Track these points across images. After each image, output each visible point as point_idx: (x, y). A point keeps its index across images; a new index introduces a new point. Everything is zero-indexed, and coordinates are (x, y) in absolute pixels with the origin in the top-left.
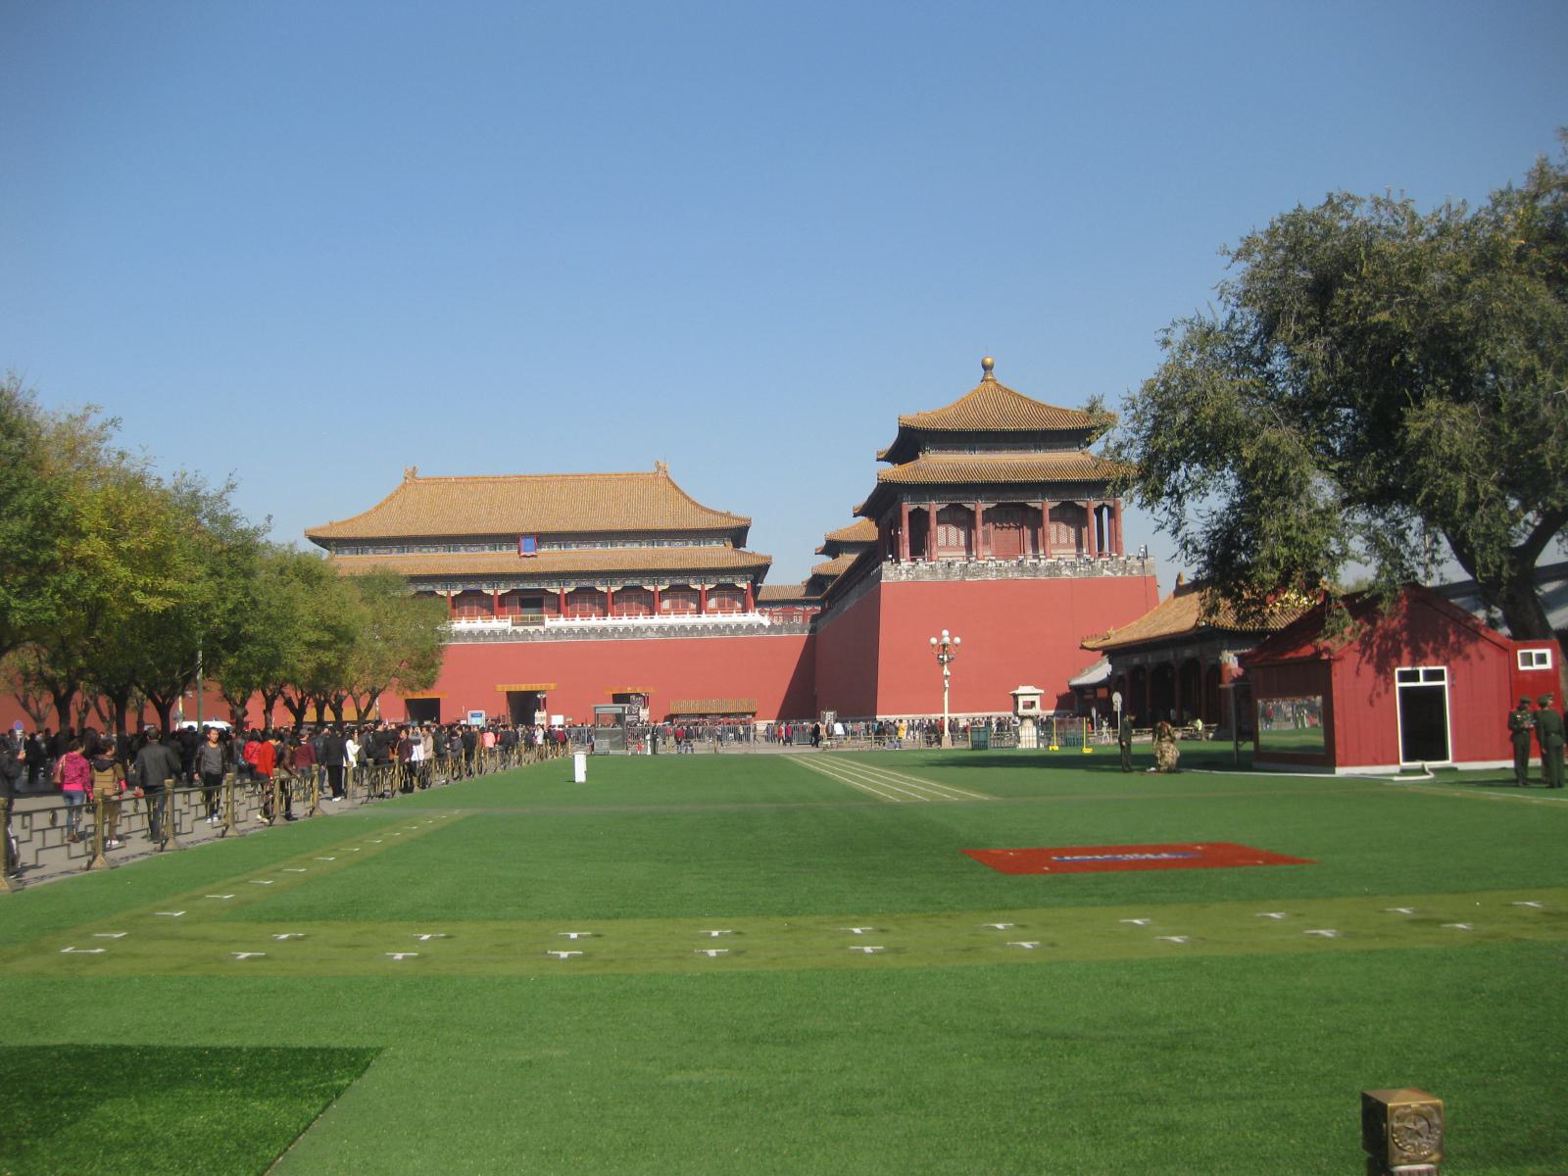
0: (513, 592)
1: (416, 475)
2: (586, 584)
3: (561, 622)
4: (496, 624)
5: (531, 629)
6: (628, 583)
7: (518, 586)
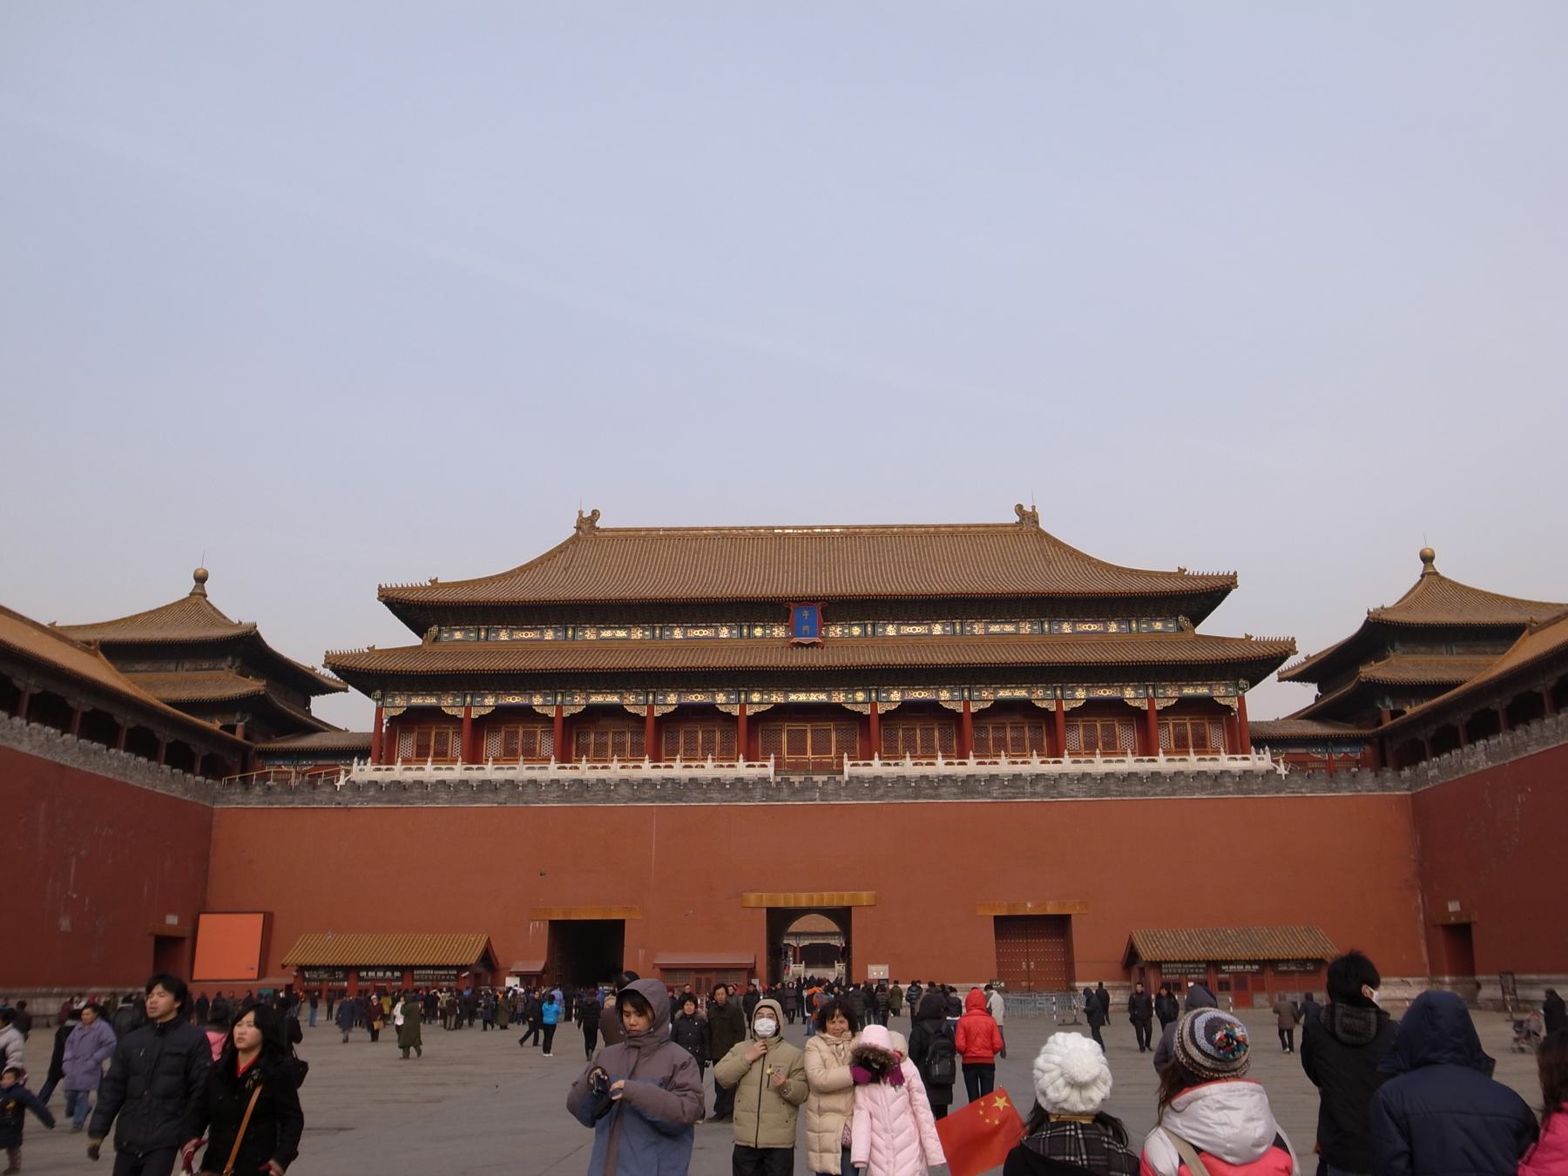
3: (877, 767)
4: (742, 769)
5: (820, 779)
6: (1004, 694)
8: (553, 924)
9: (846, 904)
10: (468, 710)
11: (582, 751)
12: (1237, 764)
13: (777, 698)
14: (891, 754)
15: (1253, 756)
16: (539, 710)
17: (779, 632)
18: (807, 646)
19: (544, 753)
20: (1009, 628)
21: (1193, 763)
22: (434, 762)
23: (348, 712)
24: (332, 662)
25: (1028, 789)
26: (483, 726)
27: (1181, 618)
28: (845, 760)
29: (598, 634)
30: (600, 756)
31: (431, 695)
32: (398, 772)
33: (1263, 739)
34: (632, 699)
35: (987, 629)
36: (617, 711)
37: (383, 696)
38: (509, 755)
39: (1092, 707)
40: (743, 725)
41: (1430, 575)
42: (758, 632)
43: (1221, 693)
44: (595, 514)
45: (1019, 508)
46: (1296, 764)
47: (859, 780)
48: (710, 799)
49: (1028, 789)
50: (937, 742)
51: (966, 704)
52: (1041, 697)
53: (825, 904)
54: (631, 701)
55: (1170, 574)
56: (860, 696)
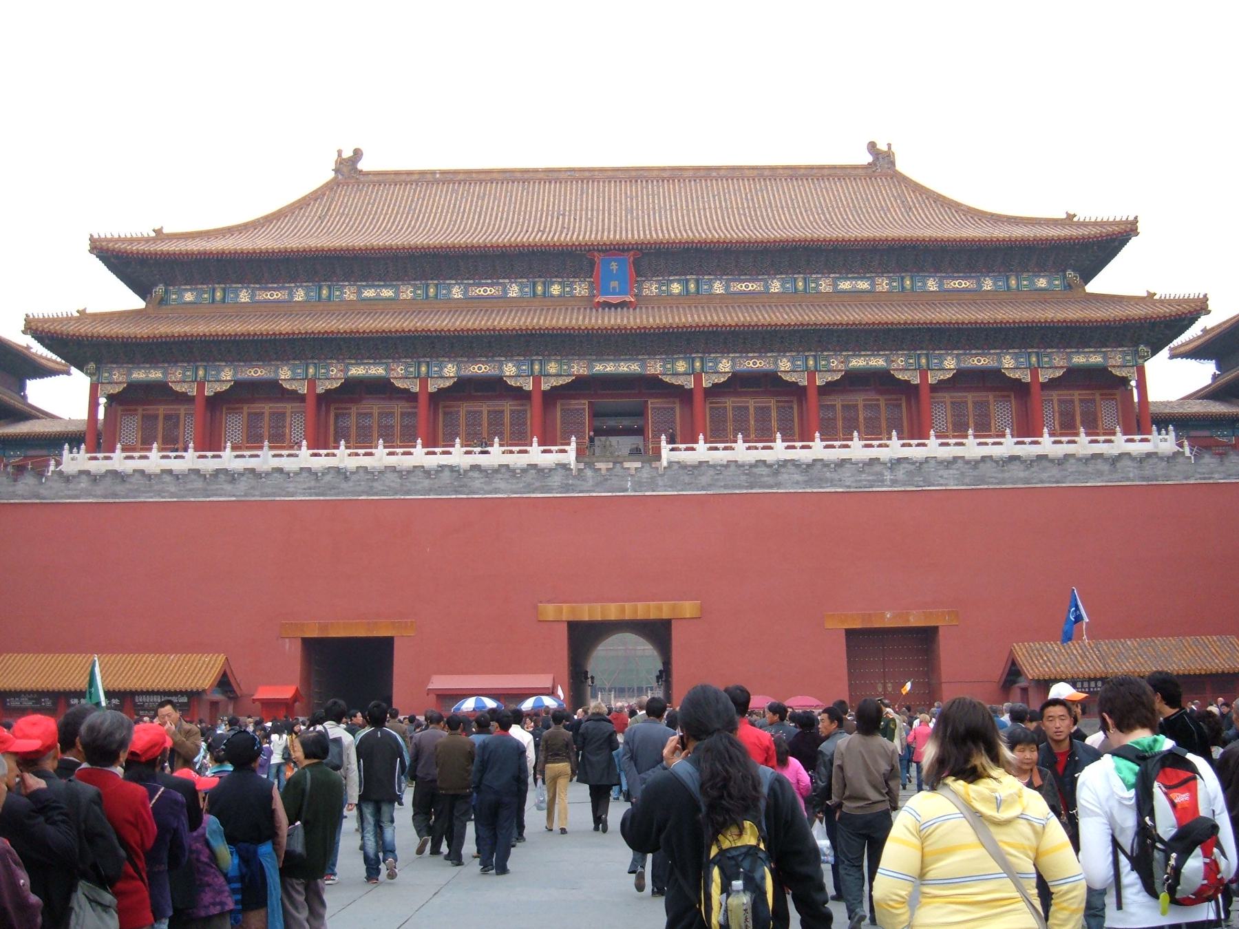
0: (580, 386)
1: (363, 165)
2: (754, 364)
3: (701, 451)
4: (536, 454)
6: (858, 363)
7: (590, 367)
8: (307, 642)
9: (665, 616)
10: (201, 386)
12: (1138, 447)
13: (579, 368)
14: (718, 435)
15: (1154, 436)
16: (287, 386)
17: (581, 289)
18: (616, 306)
19: (295, 437)
20: (863, 285)
21: (1083, 445)
22: (161, 450)
23: (64, 397)
24: (34, 328)
25: (888, 476)
26: (216, 403)
27: (1070, 274)
28: (663, 443)
29: (359, 293)
30: (363, 440)
31: (155, 368)
32: (118, 461)
33: (1163, 421)
34: (400, 370)
35: (835, 285)
36: (382, 388)
37: (98, 369)
38: (252, 441)
40: (537, 400)
42: (555, 290)
43: (1115, 360)
44: (358, 154)
45: (872, 147)
46: (1202, 447)
47: (683, 466)
48: (496, 491)
49: (888, 476)
50: (774, 424)
51: (812, 375)
52: (902, 366)
53: (641, 615)
54: (400, 373)
55: (1055, 222)
56: (681, 366)
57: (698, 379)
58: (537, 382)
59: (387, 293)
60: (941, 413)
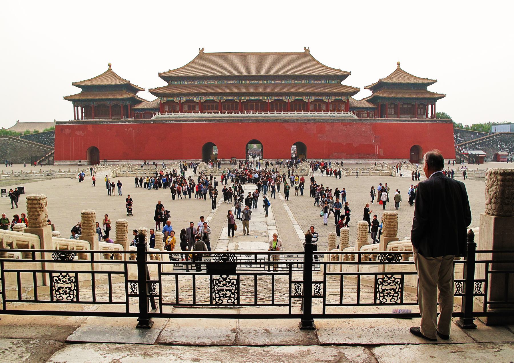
1: (204, 51)
6: (297, 98)
11: (205, 109)
12: (345, 115)
13: (247, 98)
15: (349, 113)
20: (300, 82)
30: (209, 110)
32: (166, 115)
38: (189, 112)
39: (316, 100)
41: (399, 69)
42: (243, 82)
44: (203, 49)
45: (305, 48)
52: (305, 99)
54: (216, 99)
56: (266, 98)
57: (268, 100)
58: (240, 100)
59: (213, 82)
60: (312, 107)
